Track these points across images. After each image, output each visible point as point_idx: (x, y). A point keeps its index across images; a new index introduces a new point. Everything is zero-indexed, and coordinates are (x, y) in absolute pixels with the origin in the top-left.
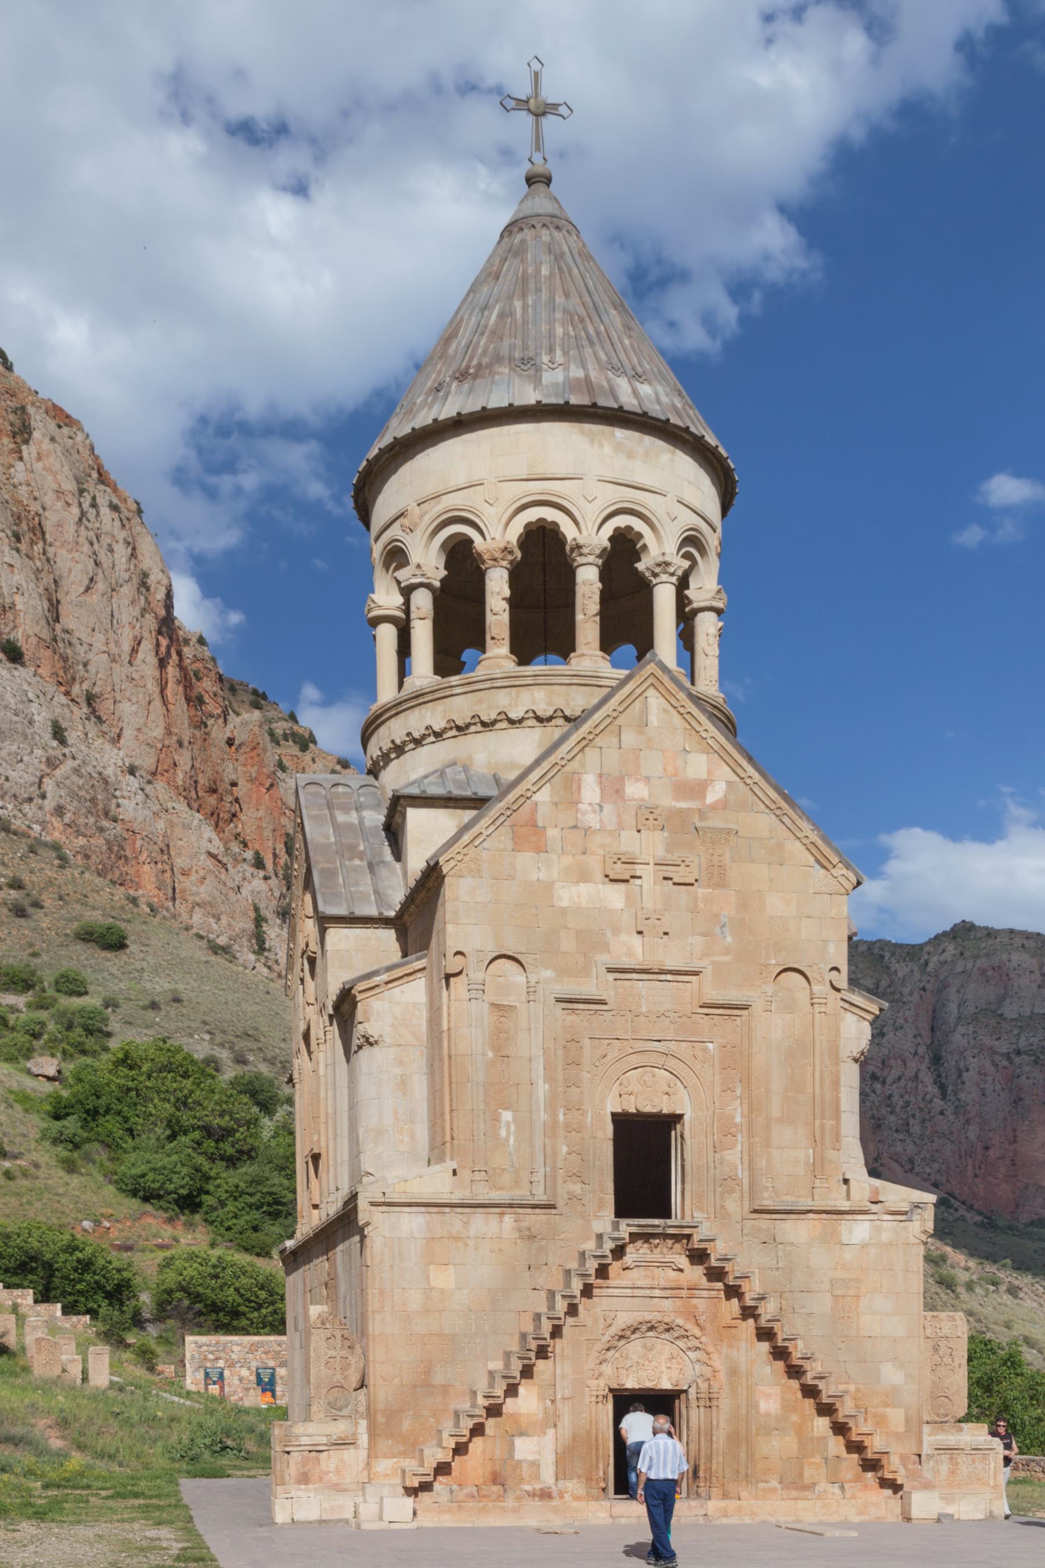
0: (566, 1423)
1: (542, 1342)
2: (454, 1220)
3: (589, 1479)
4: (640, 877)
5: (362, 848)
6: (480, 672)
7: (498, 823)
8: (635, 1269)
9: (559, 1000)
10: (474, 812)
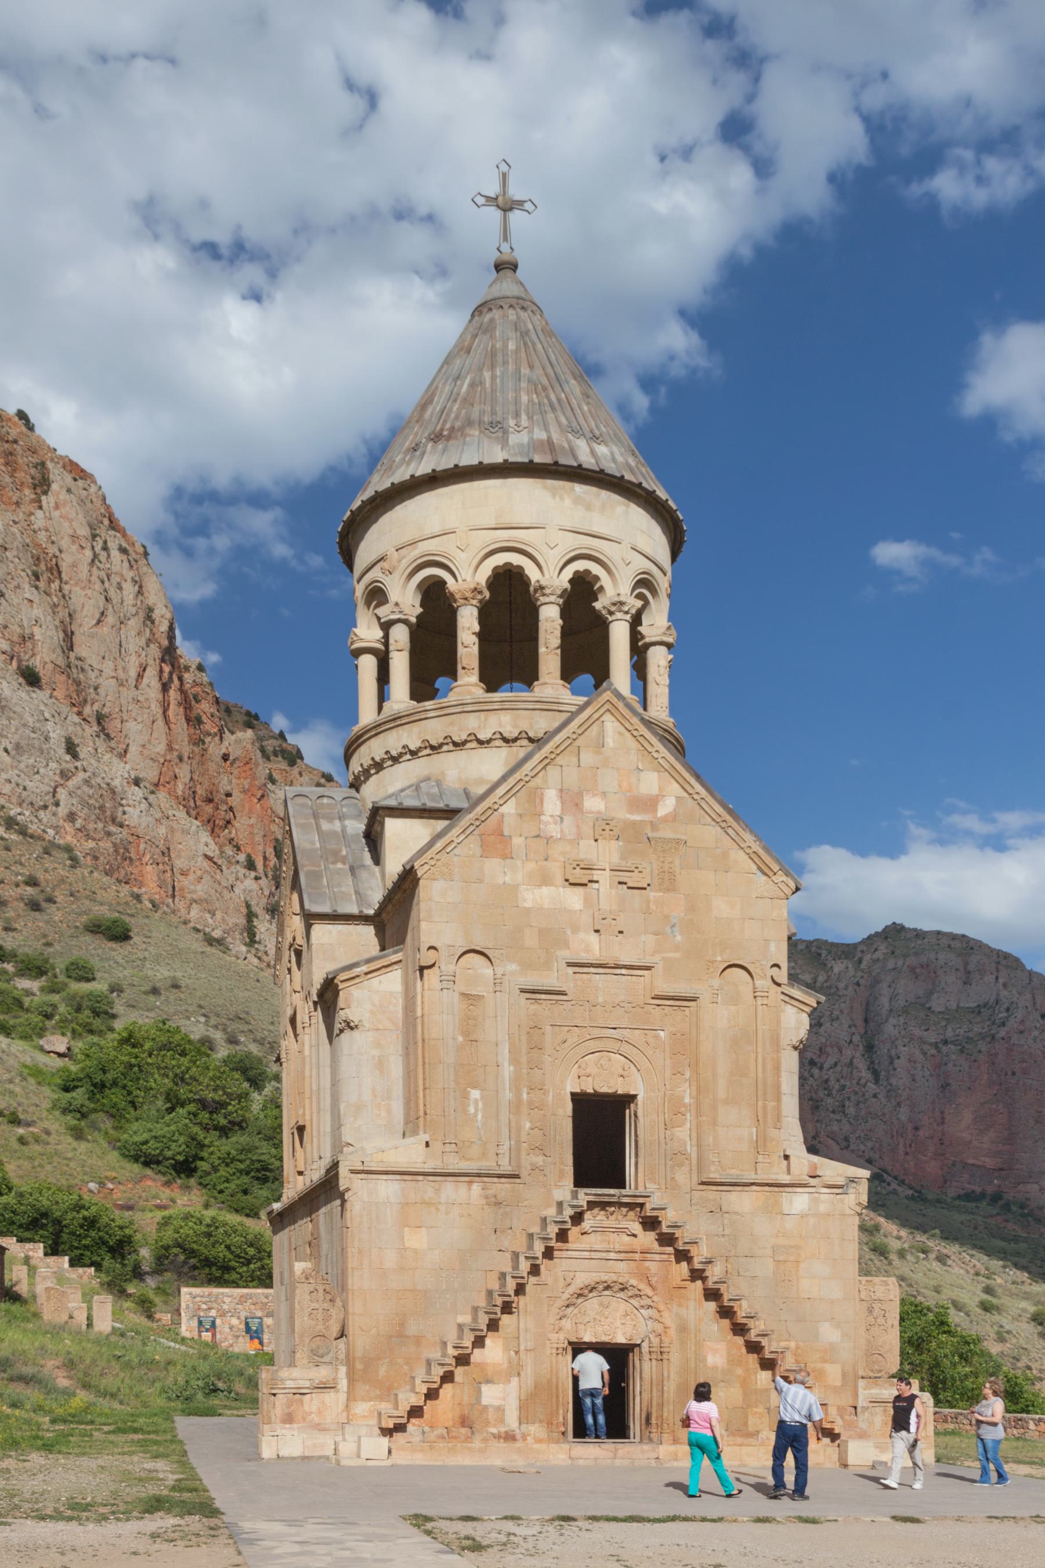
0: (528, 1372)
1: (507, 1299)
2: (427, 1188)
3: (550, 1423)
4: (597, 882)
5: (344, 853)
6: (452, 698)
9: (523, 991)
10: (446, 823)
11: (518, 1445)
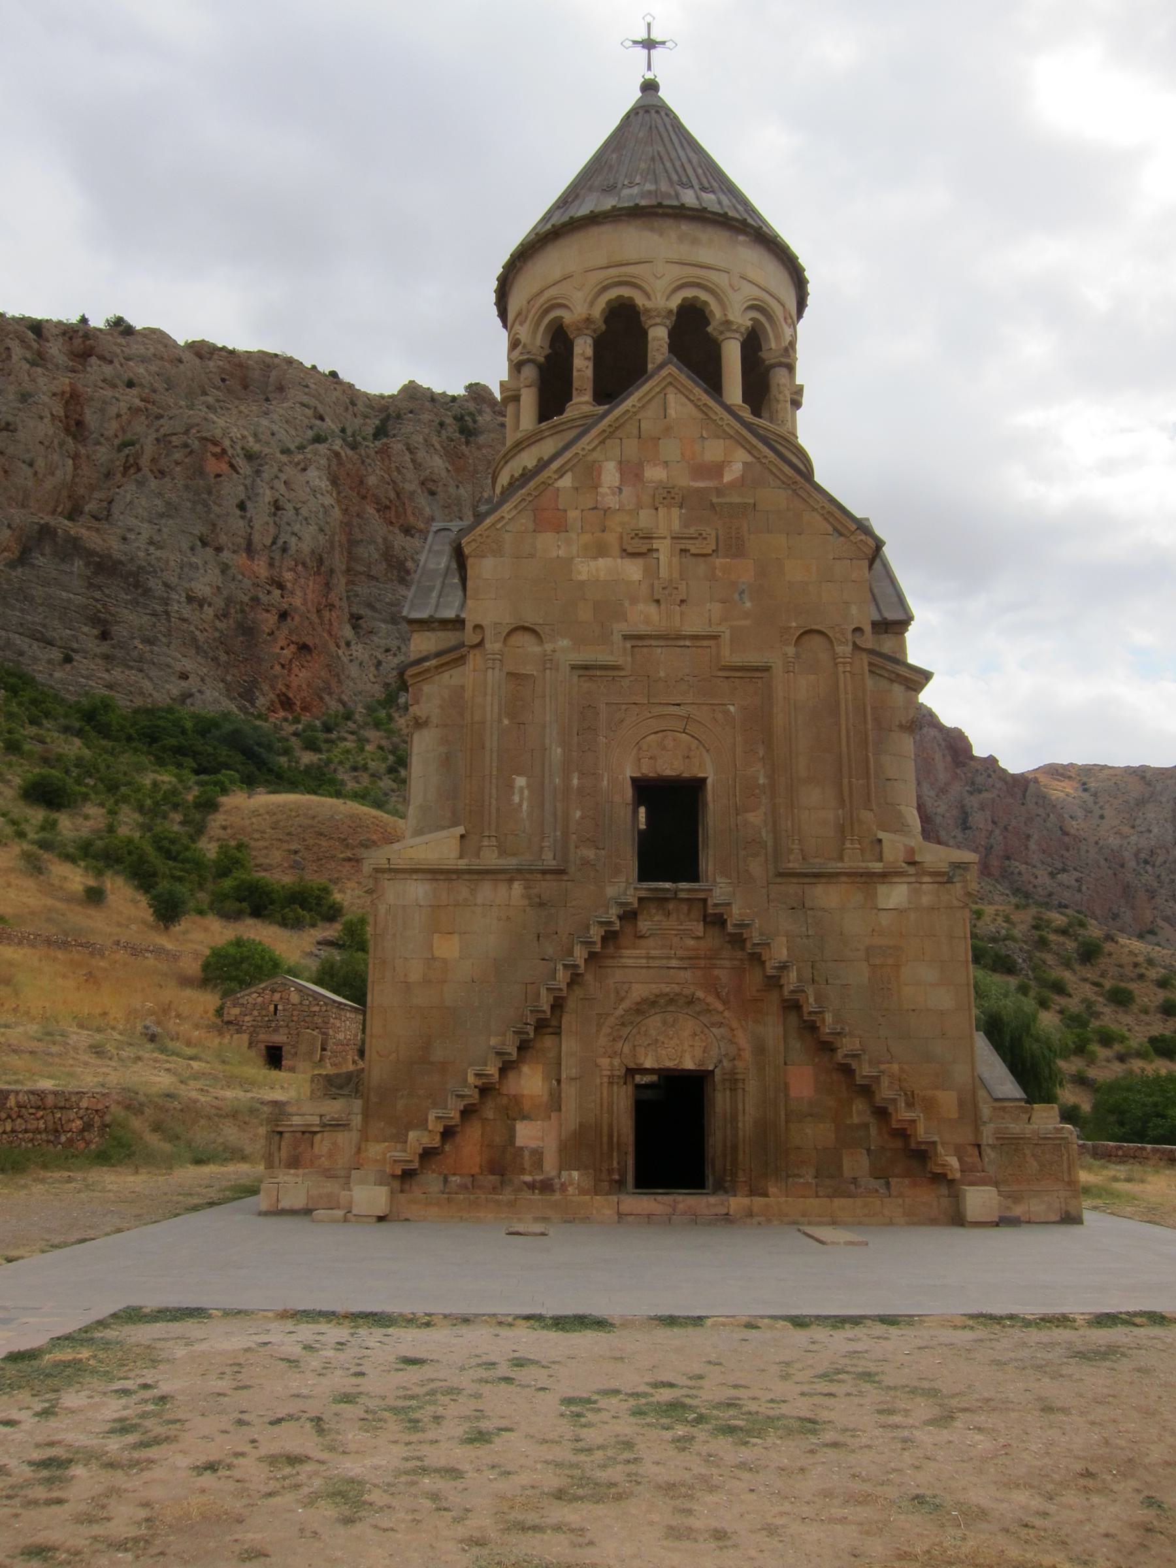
11: (557, 1196)
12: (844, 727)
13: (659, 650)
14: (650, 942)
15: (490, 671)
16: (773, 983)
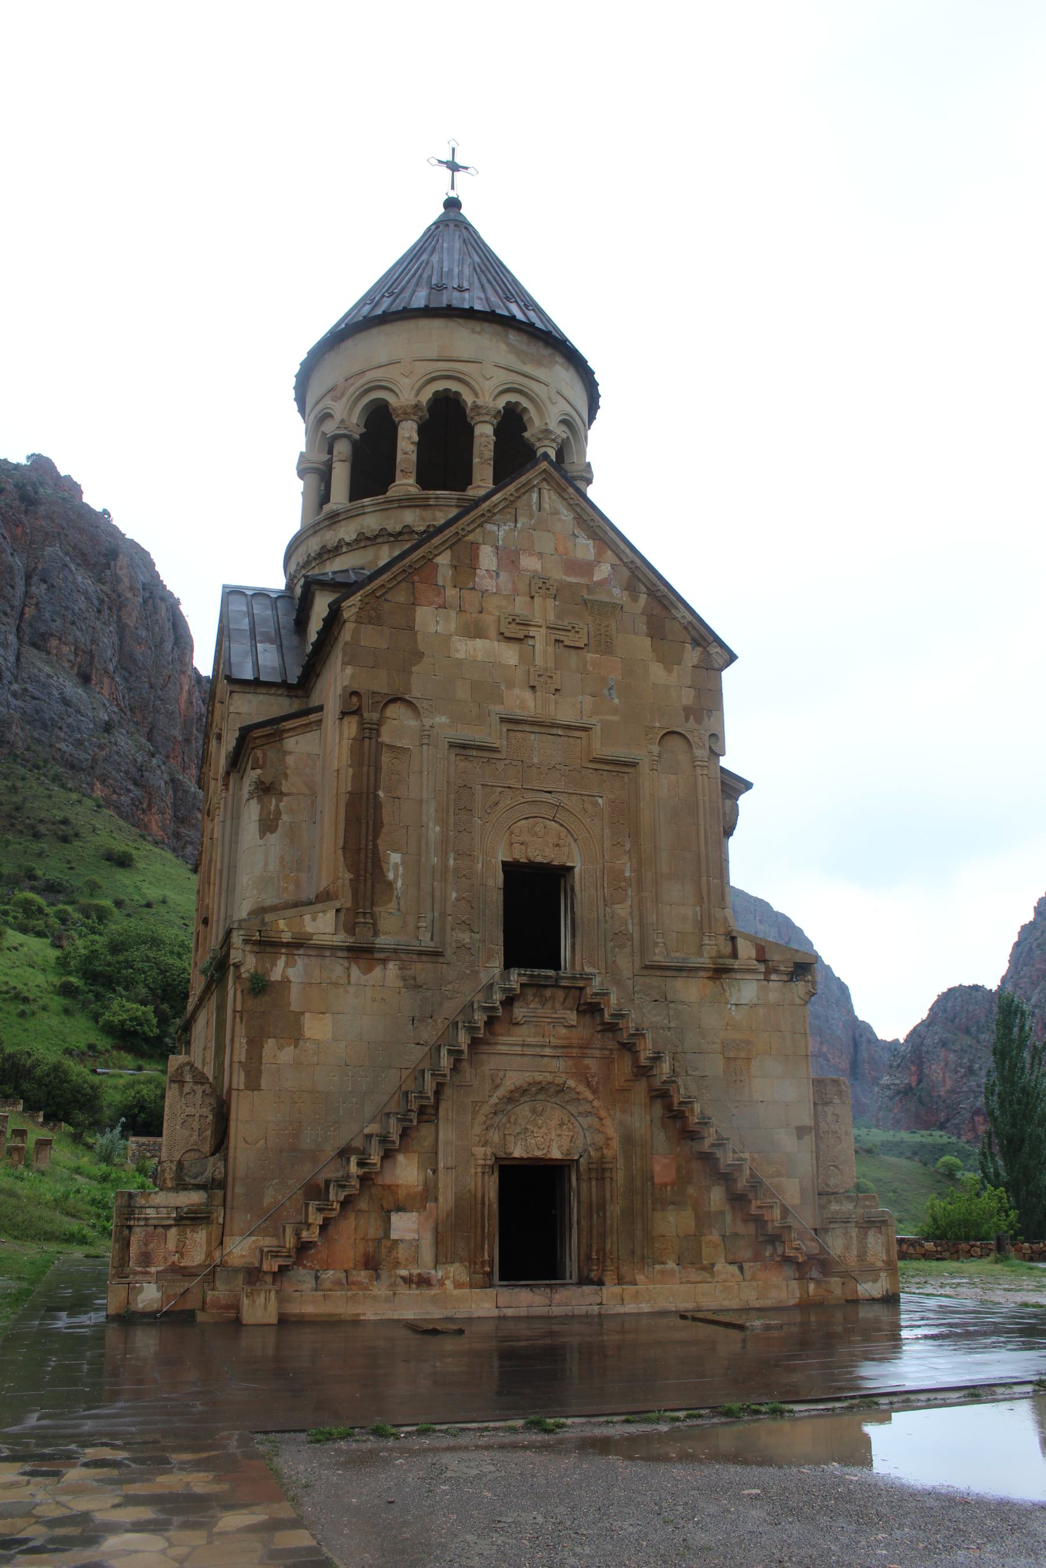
3: (472, 1262)
7: (399, 579)
8: (525, 1026)
12: (702, 827)
13: (533, 736)
14: (524, 1030)
15: (367, 741)
16: (643, 1072)
